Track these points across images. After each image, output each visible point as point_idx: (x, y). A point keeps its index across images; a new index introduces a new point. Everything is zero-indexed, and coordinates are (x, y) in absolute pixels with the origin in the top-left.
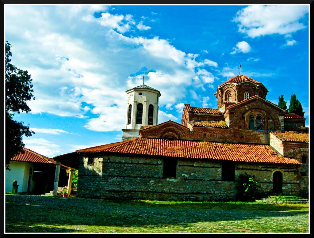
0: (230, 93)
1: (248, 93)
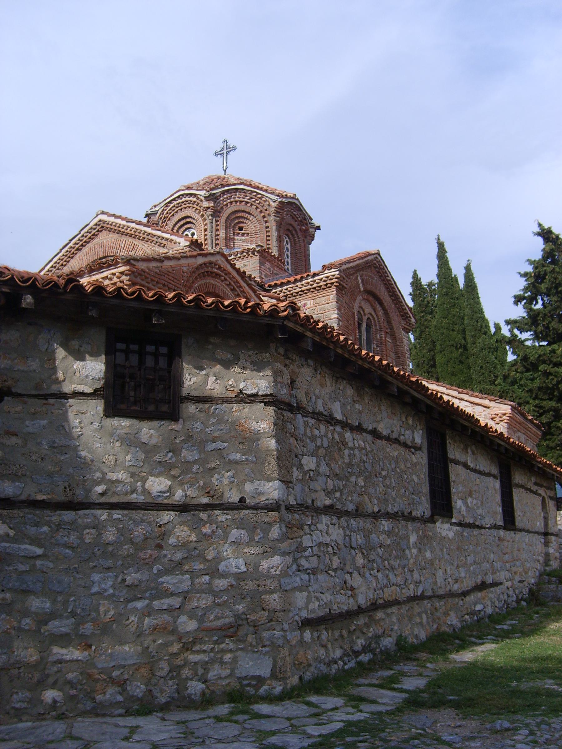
0: (243, 223)
1: (288, 239)
